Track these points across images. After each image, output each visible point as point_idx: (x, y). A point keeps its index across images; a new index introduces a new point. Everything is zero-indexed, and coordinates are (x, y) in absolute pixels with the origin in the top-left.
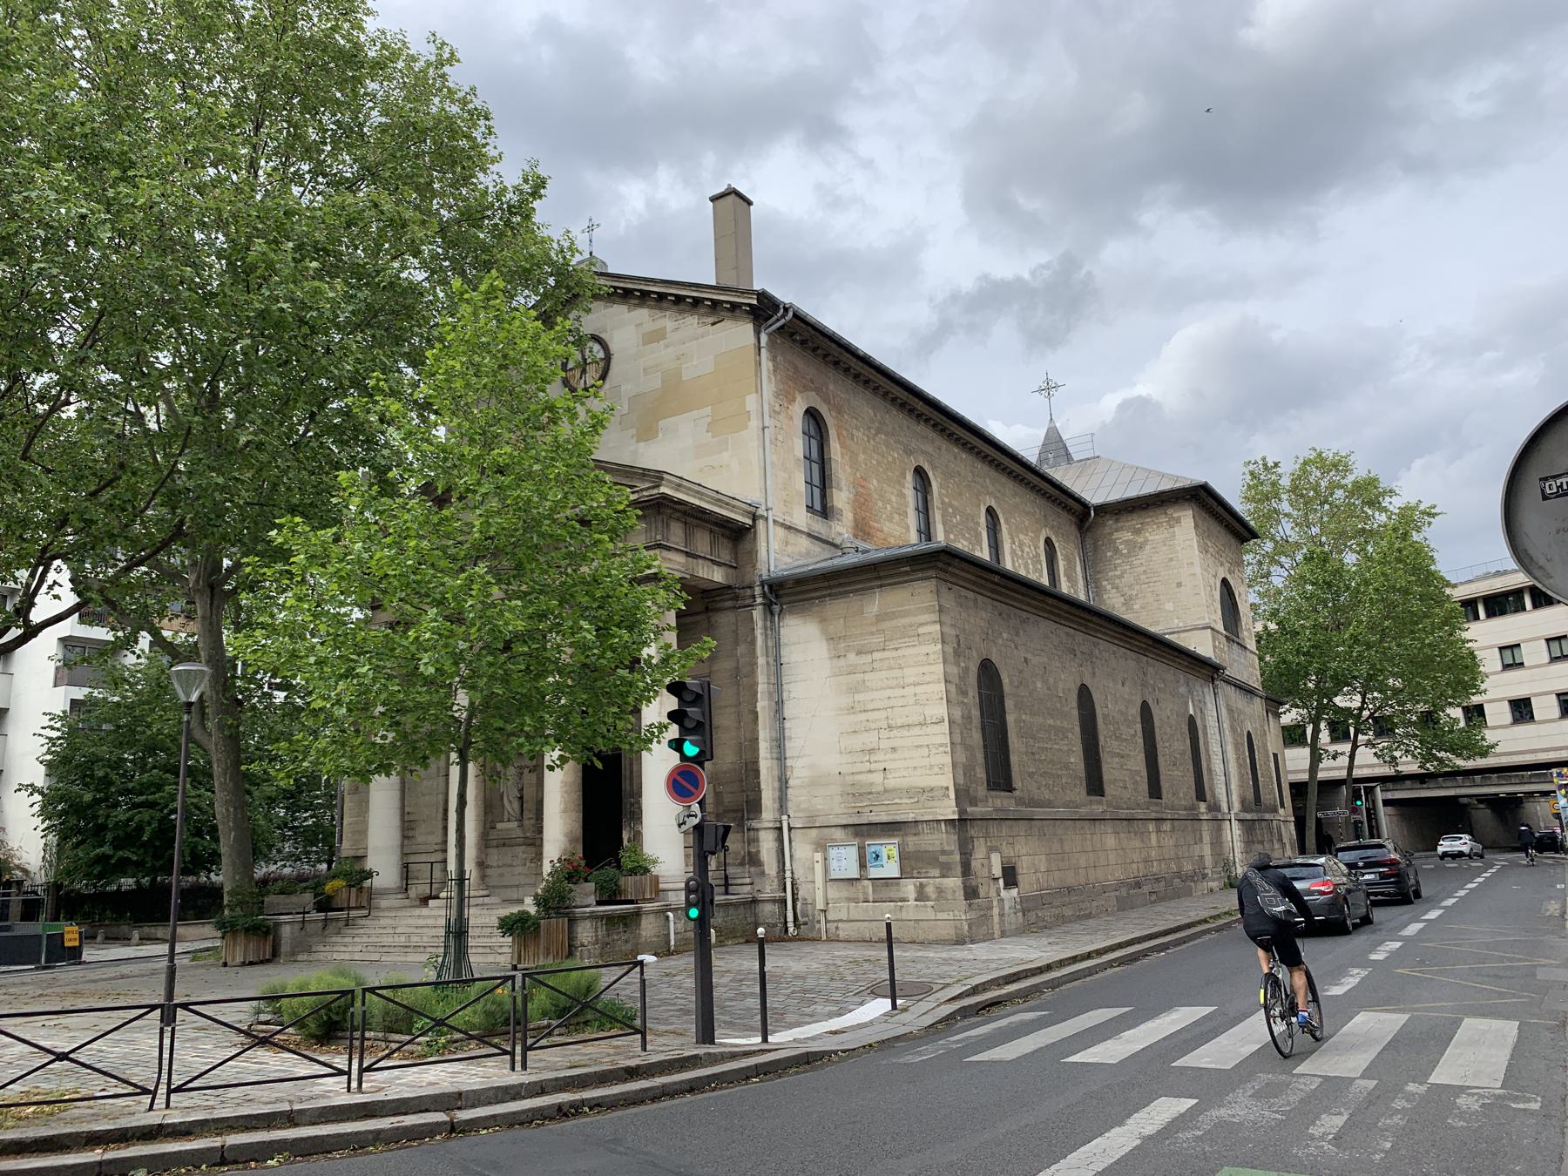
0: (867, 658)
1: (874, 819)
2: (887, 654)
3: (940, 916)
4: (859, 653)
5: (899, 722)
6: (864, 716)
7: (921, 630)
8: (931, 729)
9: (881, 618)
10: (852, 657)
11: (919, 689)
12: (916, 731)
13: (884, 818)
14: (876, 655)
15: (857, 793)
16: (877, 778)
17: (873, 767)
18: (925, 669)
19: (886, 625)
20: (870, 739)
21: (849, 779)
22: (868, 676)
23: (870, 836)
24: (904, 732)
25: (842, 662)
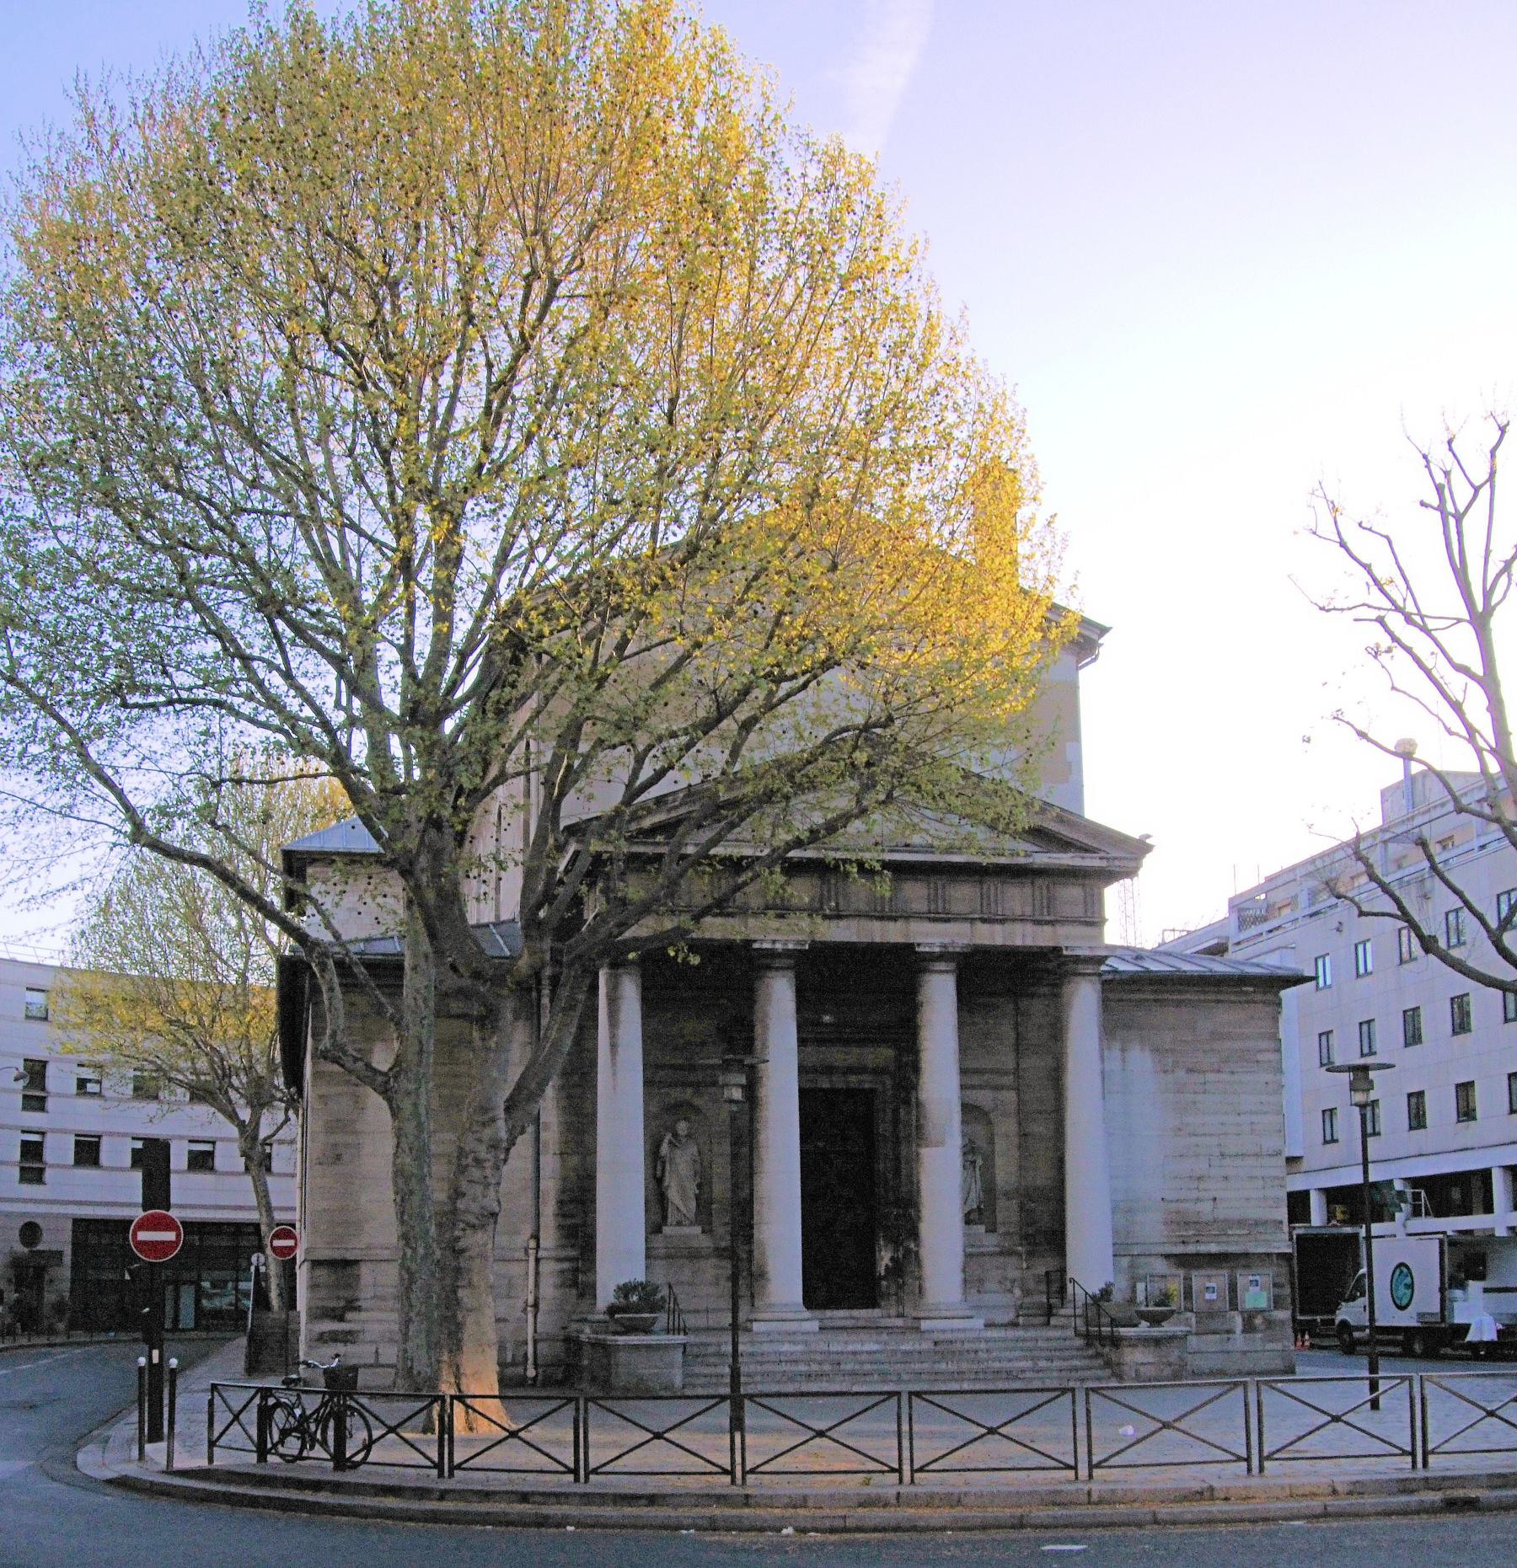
0: (1200, 1078)
1: (1203, 1249)
2: (1224, 1077)
3: (1269, 1346)
4: (1190, 1071)
5: (1233, 1150)
6: (1194, 1140)
7: (1260, 1057)
8: (1266, 1161)
9: (1216, 1036)
10: (1181, 1074)
11: (1255, 1118)
12: (1250, 1161)
13: (1214, 1248)
14: (1210, 1077)
15: (1181, 1222)
16: (1206, 1207)
17: (1202, 1194)
18: (1264, 1098)
19: (1217, 1045)
20: (1201, 1167)
21: (1173, 1206)
22: (1199, 1098)
23: (1197, 1267)
24: (1239, 1162)
25: (1170, 1077)
